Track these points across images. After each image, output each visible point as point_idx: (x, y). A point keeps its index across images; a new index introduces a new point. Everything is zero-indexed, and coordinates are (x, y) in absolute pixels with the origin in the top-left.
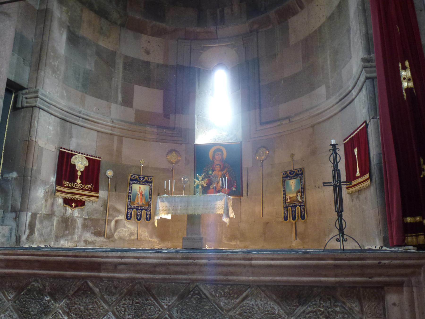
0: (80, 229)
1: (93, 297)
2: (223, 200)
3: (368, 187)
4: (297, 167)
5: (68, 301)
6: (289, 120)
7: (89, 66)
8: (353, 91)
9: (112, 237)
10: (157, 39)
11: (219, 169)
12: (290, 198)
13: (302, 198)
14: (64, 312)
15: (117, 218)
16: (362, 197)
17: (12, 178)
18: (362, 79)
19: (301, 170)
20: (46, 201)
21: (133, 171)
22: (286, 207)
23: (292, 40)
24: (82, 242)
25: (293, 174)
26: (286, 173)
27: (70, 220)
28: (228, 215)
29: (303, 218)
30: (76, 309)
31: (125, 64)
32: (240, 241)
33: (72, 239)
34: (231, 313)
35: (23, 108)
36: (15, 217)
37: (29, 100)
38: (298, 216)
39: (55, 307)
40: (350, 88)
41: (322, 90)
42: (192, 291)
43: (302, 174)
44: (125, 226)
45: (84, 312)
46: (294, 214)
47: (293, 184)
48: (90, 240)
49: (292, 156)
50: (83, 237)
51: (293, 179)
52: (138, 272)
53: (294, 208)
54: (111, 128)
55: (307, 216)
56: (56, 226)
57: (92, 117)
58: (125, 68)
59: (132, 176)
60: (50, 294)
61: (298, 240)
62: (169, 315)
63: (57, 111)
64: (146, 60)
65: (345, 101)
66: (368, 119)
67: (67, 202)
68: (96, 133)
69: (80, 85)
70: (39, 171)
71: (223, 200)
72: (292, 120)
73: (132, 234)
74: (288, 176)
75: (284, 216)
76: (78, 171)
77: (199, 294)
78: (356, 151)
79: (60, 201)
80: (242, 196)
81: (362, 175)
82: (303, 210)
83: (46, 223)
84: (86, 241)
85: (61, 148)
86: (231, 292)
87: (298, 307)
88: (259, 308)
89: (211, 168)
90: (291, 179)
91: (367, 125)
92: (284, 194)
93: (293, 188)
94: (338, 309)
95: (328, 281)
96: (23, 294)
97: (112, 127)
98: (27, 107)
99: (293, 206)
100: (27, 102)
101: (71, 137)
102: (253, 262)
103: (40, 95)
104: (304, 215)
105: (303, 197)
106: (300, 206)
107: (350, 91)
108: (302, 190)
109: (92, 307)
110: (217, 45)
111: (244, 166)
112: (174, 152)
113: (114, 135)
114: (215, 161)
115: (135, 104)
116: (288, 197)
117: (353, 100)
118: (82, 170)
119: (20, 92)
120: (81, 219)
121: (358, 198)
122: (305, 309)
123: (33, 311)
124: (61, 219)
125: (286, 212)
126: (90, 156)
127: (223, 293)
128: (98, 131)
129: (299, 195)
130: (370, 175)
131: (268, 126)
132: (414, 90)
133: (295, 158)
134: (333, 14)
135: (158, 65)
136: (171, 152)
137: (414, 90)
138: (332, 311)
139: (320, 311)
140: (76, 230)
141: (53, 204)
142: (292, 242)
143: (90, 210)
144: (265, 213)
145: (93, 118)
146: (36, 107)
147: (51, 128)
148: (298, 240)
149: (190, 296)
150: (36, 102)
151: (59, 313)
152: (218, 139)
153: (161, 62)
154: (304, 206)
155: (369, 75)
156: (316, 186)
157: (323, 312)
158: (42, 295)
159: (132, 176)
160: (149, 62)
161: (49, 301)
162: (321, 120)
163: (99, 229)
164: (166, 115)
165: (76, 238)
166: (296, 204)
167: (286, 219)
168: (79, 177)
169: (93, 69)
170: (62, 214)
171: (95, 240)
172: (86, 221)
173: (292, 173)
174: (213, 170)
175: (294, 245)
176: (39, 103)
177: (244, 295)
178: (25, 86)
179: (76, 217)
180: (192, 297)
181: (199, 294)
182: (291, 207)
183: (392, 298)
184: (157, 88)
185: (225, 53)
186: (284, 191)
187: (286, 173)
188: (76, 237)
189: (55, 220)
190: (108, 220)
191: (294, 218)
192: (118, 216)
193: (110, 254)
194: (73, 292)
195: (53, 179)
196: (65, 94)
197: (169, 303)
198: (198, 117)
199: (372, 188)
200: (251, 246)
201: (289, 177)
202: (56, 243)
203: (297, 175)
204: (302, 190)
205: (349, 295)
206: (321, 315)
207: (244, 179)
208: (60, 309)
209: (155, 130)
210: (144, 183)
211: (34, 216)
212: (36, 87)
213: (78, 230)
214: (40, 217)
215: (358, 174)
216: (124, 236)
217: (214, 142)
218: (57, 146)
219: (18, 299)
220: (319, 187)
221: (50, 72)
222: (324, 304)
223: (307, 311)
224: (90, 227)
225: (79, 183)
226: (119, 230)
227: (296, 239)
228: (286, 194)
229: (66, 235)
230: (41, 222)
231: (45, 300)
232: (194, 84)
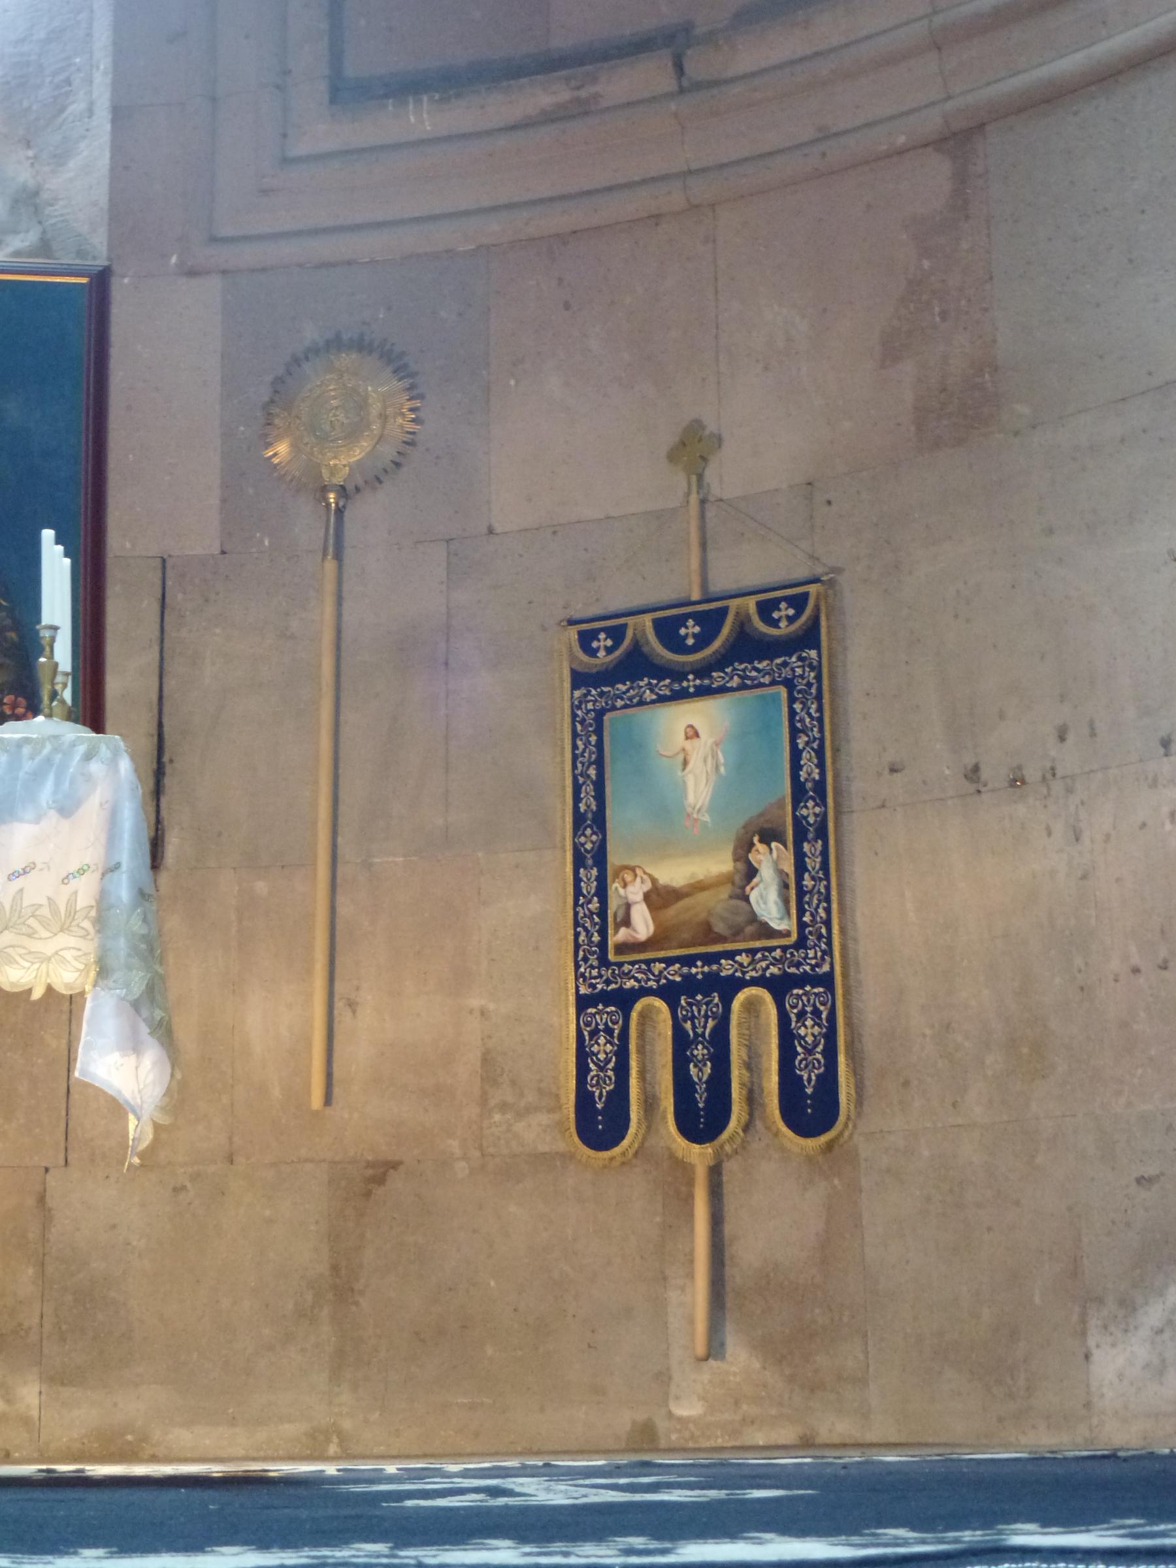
4: (748, 566)
6: (679, 68)
12: (659, 898)
13: (798, 893)
19: (798, 603)
22: (606, 999)
25: (703, 641)
26: (617, 634)
29: (810, 1108)
32: (56, 1378)
38: (753, 1099)
43: (810, 637)
46: (700, 1073)
47: (699, 751)
49: (694, 449)
51: (704, 692)
53: (701, 1016)
55: (860, 1101)
61: (740, 1356)
72: (698, 65)
74: (633, 661)
75: (584, 1099)
82: (808, 1031)
90: (680, 696)
92: (593, 862)
93: (698, 788)
99: (690, 986)
104: (829, 1081)
105: (810, 889)
106: (779, 987)
108: (806, 819)
116: (631, 891)
125: (603, 1048)
129: (767, 873)
131: (422, 118)
133: (728, 476)
142: (663, 1378)
144: (357, 1053)
148: (740, 1356)
154: (827, 981)
156: (973, 773)
162: (1070, 64)
166: (727, 968)
167: (600, 1122)
173: (691, 629)
175: (688, 1409)
182: (669, 993)
186: (591, 820)
187: (617, 634)
191: (702, 1116)
200: (182, 1437)
201: (660, 671)
203: (747, 647)
204: (806, 819)
220: (1017, 781)
227: (715, 1349)
228: (614, 859)
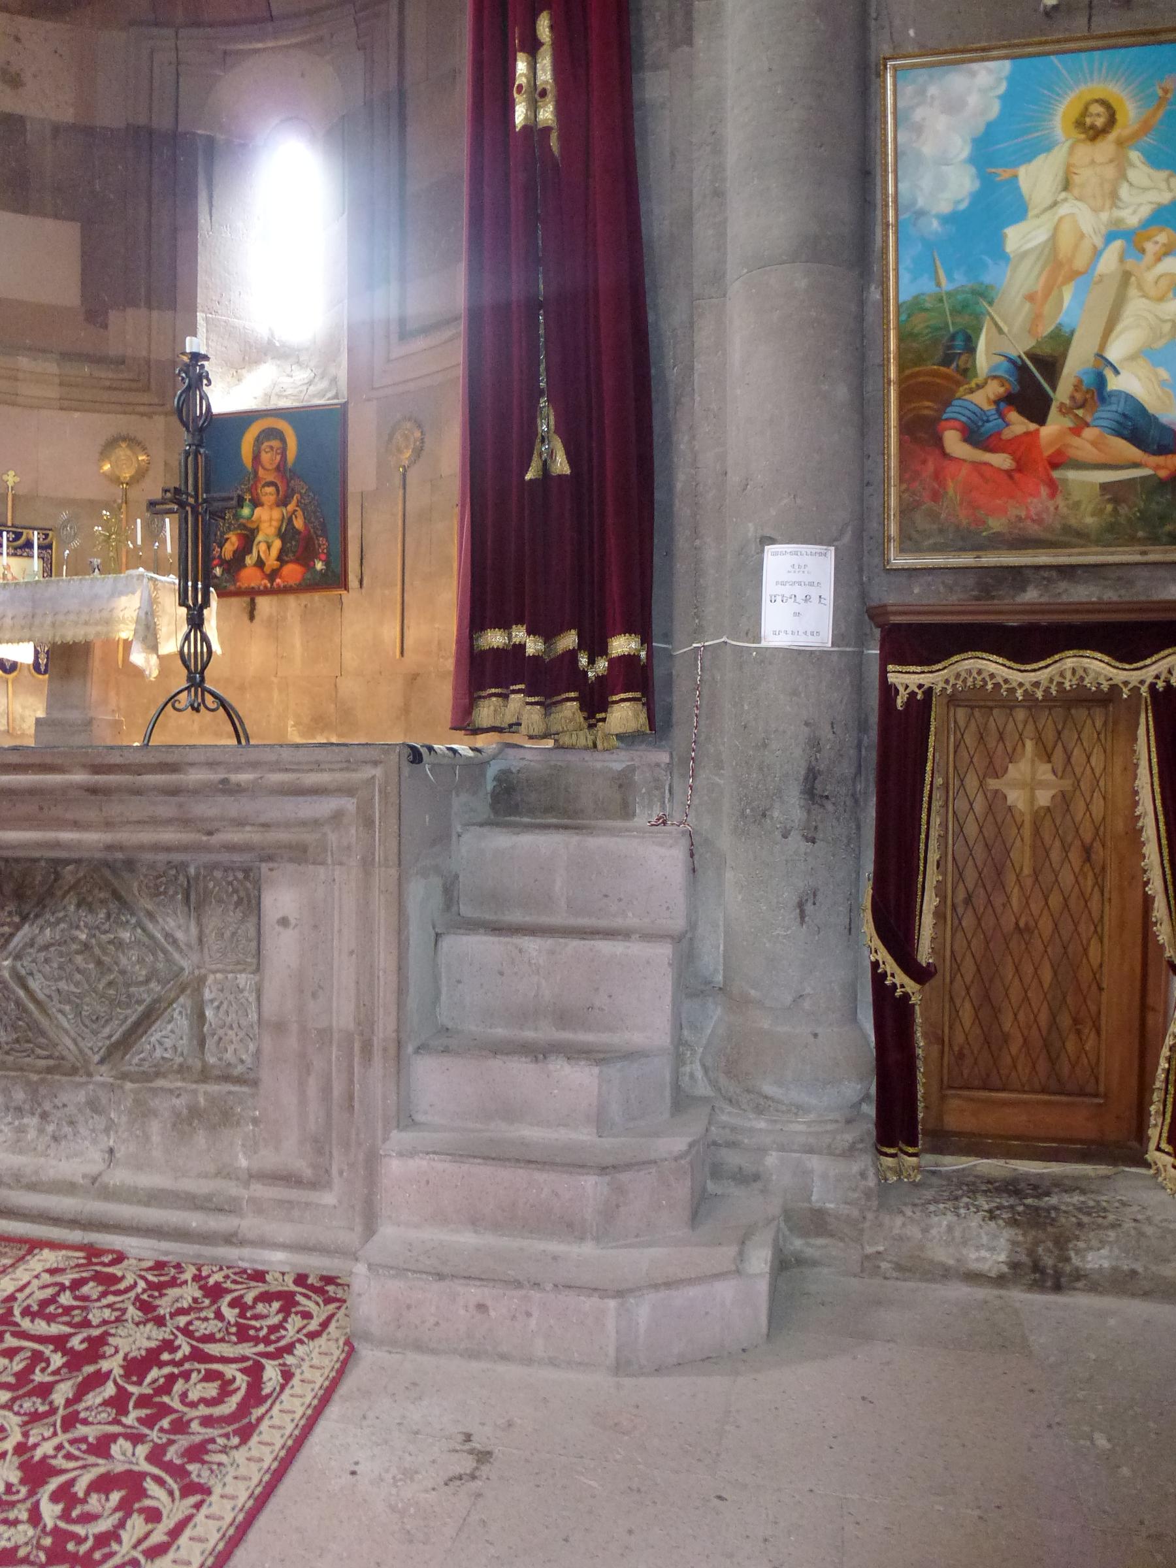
2: (138, 594)
10: (49, 25)
11: (273, 498)
28: (152, 645)
64: (8, 110)
71: (138, 594)
80: (346, 588)
87: (18, 928)
94: (126, 935)
95: (79, 841)
110: (270, 44)
111: (353, 488)
112: (124, 445)
114: (261, 472)
132: (554, 136)
135: (57, 129)
136: (111, 445)
137: (554, 136)
138: (110, 942)
139: (74, 939)
144: (409, 642)
152: (279, 396)
153: (68, 115)
157: (86, 946)
160: (21, 119)
164: (94, 313)
174: (256, 503)
183: (282, 899)
184: (56, 216)
185: (303, 75)
198: (207, 320)
205: (162, 889)
206: (78, 952)
207: (353, 532)
209: (52, 368)
210: (19, 552)
217: (264, 408)
222: (90, 919)
223: (40, 941)
232: (191, 196)
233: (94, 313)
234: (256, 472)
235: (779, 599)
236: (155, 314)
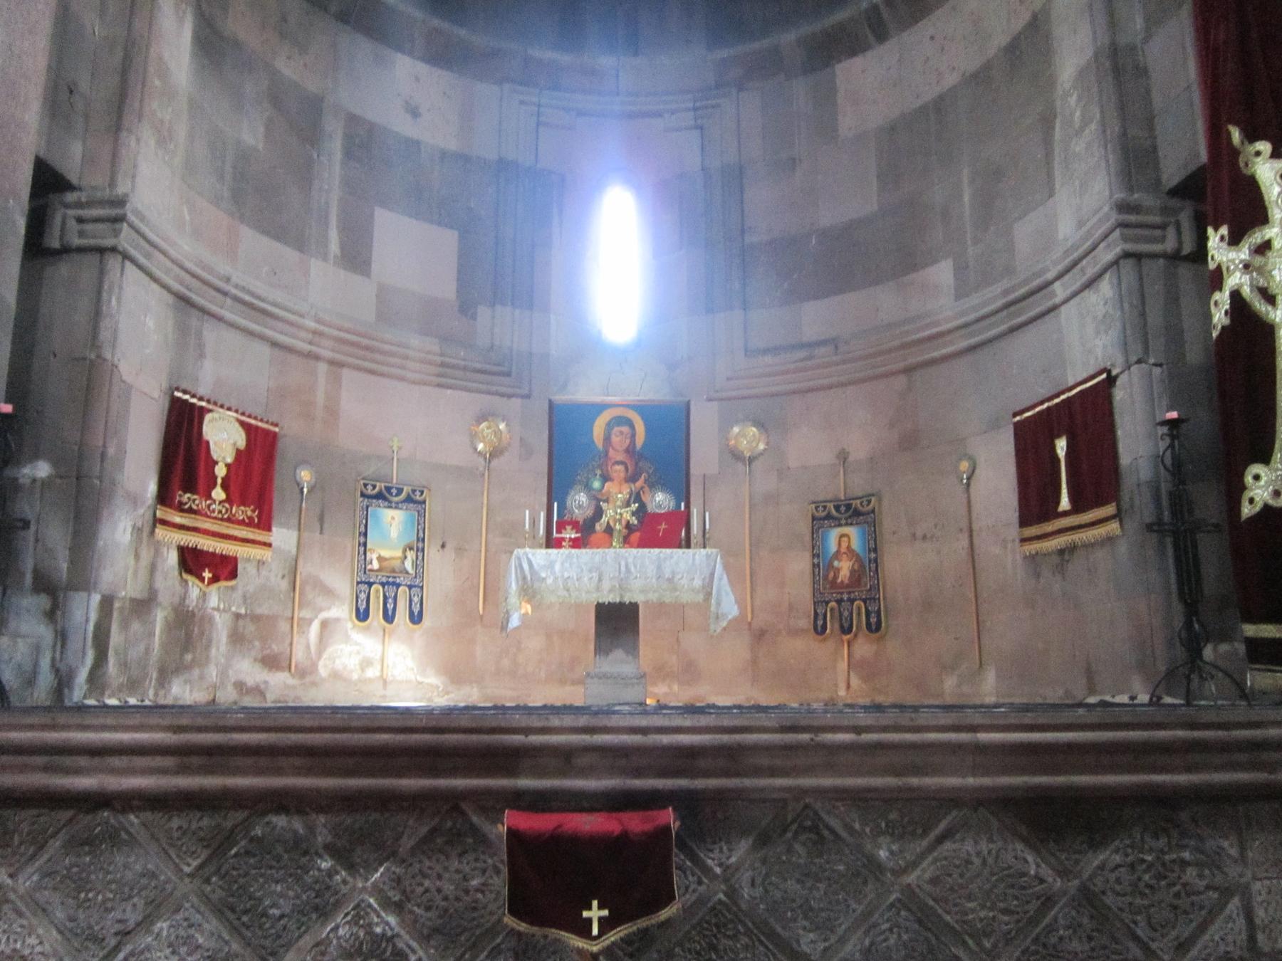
0: (223, 648)
1: (483, 853)
3: (1110, 540)
5: (398, 870)
7: (251, 132)
8: (1057, 284)
9: (311, 673)
11: (622, 475)
14: (387, 904)
15: (324, 615)
16: (1077, 565)
17: (34, 480)
18: (1106, 255)
20: (137, 556)
21: (370, 469)
23: (848, 123)
24: (230, 688)
27: (196, 619)
30: (427, 891)
31: (348, 138)
33: (202, 677)
34: (911, 878)
35: (66, 250)
36: (48, 607)
37: (89, 227)
39: (354, 888)
40: (1050, 276)
41: (942, 273)
42: (792, 823)
44: (347, 639)
45: (458, 899)
48: (250, 682)
50: (231, 672)
52: (638, 773)
54: (310, 336)
56: (161, 638)
57: (259, 298)
58: (348, 154)
59: (365, 485)
60: (331, 850)
62: (726, 894)
63: (167, 272)
65: (1028, 308)
66: (1120, 360)
67: (192, 561)
68: (264, 350)
69: (226, 194)
70: (119, 463)
73: (366, 663)
76: (216, 463)
77: (815, 829)
78: (1061, 445)
79: (173, 557)
81: (1077, 508)
83: (136, 626)
84: (240, 686)
85: (177, 389)
86: (906, 820)
88: (984, 862)
89: (599, 472)
91: (1111, 380)
94: (1186, 855)
96: (236, 855)
97: (315, 332)
98: (81, 250)
100: (81, 234)
101: (202, 356)
102: (983, 737)
103: (131, 217)
107: (1049, 284)
109: (483, 884)
111: (696, 471)
113: (317, 358)
114: (611, 453)
115: (375, 267)
117: (1054, 308)
118: (229, 460)
119: (53, 198)
120: (227, 616)
121: (1061, 569)
122: (1107, 859)
123: (273, 906)
124: (173, 616)
126: (250, 416)
127: (883, 825)
128: (275, 344)
130: (1118, 506)
134: (987, 66)
135: (444, 155)
138: (1174, 861)
139: (1143, 861)
140: (213, 651)
141: (153, 568)
143: (251, 588)
145: (263, 300)
146: (114, 250)
147: (151, 323)
149: (789, 835)
150: (117, 233)
151: (370, 906)
153: (453, 145)
155: (1130, 247)
156: (914, 535)
157: (1150, 866)
158: (306, 853)
159: (365, 485)
160: (418, 143)
161: (331, 873)
162: (936, 354)
163: (274, 647)
164: (466, 308)
165: (214, 674)
168: (219, 481)
169: (261, 146)
170: (176, 600)
171: (266, 682)
172: (241, 623)
174: (606, 478)
176: (125, 239)
177: (943, 826)
178: (75, 181)
179: (213, 609)
180: (796, 833)
181: (815, 829)
184: (439, 224)
188: (212, 672)
189: (160, 617)
190: (299, 619)
192: (329, 608)
193: (555, 722)
194: (412, 843)
195: (152, 488)
196: (187, 218)
197: (728, 858)
199: (1123, 548)
202: (162, 693)
206: (1145, 871)
208: (371, 895)
211: (107, 603)
212: (112, 184)
213: (218, 649)
214: (122, 609)
215: (1065, 503)
216: (345, 667)
218: (165, 385)
219: (217, 872)
221: (152, 142)
222: (1154, 843)
223: (1111, 865)
224: (250, 642)
225: (221, 502)
226: (330, 650)
229: (188, 668)
230: (125, 625)
231: (319, 869)
233: (466, 308)
234: (606, 453)
235: (816, 561)
236: (517, 312)
